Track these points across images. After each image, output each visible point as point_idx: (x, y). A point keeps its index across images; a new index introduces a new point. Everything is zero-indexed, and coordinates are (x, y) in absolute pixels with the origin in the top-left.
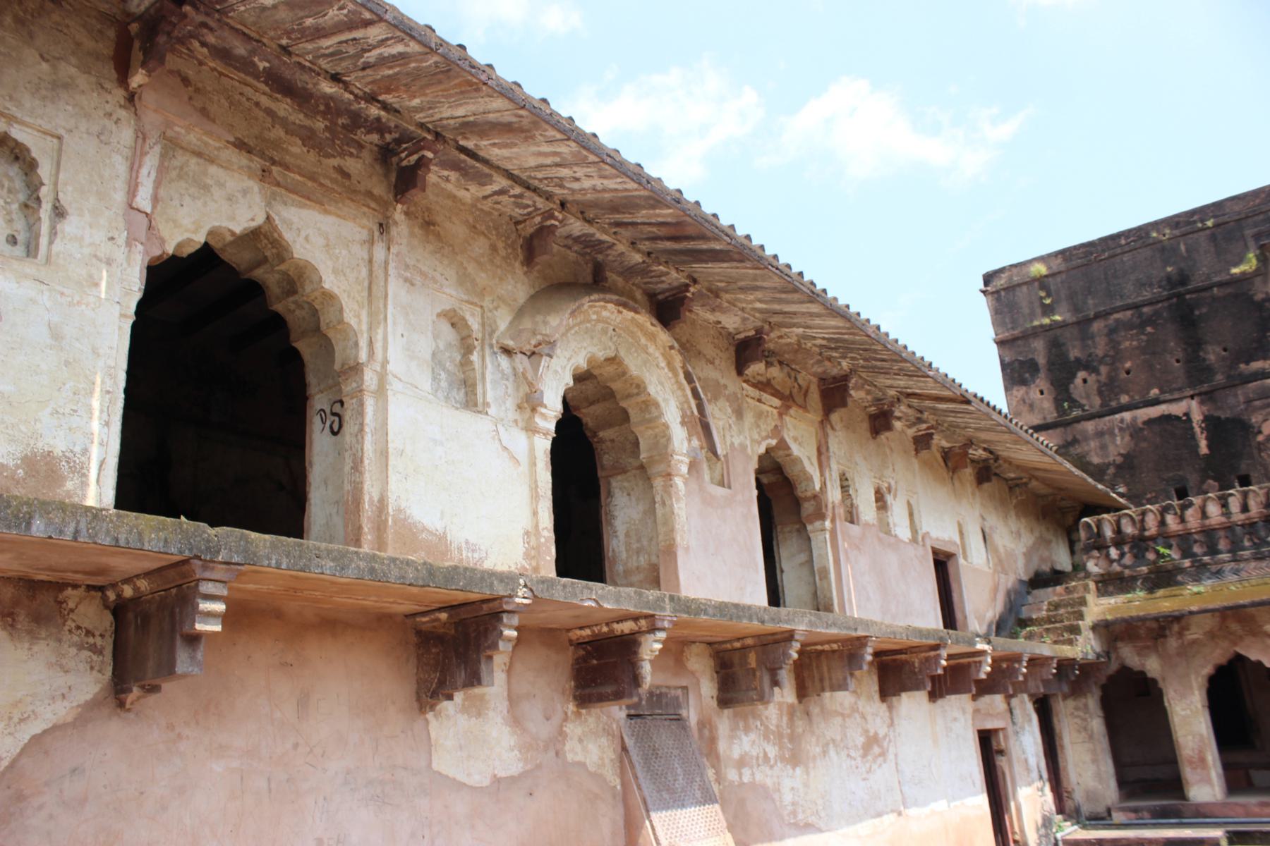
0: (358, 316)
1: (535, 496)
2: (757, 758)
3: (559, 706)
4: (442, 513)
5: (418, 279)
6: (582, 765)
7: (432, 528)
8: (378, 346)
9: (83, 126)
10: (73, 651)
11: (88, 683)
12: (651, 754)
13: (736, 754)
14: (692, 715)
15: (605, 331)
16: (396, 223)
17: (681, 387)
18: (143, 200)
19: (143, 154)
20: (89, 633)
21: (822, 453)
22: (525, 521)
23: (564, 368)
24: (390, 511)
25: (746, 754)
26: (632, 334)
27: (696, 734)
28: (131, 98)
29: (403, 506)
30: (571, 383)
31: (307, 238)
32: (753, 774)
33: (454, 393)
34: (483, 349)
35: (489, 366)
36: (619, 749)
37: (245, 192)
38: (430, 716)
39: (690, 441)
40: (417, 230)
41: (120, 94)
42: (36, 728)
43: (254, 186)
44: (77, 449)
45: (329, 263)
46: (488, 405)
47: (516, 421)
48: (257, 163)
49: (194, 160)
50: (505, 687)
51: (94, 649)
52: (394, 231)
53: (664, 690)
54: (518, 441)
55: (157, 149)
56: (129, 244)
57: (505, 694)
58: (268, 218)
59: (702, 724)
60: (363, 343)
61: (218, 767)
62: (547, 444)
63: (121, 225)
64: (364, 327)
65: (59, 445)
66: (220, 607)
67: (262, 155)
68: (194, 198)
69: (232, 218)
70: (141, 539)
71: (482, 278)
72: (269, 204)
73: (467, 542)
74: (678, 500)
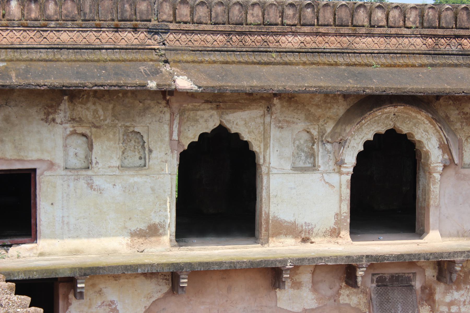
0: (260, 147)
1: (341, 200)
2: (465, 301)
3: (337, 284)
4: (294, 214)
5: (285, 125)
6: (349, 305)
7: (289, 220)
8: (267, 157)
9: (154, 119)
10: (161, 280)
11: (166, 288)
12: (388, 301)
13: (448, 299)
14: (418, 284)
15: (387, 118)
16: (274, 105)
17: (438, 131)
18: (175, 137)
19: (174, 120)
20: (165, 276)
22: (336, 210)
23: (358, 144)
24: (271, 218)
25: (455, 300)
26: (407, 113)
27: (419, 292)
28: (168, 102)
29: (276, 215)
30: (362, 149)
31: (237, 124)
32: (460, 309)
33: (309, 160)
34: (318, 143)
35: (321, 150)
36: (369, 299)
37: (211, 116)
38: (277, 290)
39: (443, 155)
40: (285, 104)
41: (164, 102)
42: (154, 299)
43: (214, 112)
44: (162, 221)
45: (247, 130)
46: (319, 167)
47: (334, 170)
48: (214, 105)
49: (192, 113)
50: (311, 279)
51: (166, 279)
52: (273, 109)
53: (400, 275)
54: (334, 178)
55: (178, 116)
56: (172, 152)
57: (311, 281)
58: (221, 121)
59: (423, 288)
60: (261, 157)
61: (202, 307)
62: (349, 177)
63: (169, 148)
64: (262, 150)
65: (157, 221)
66: (186, 280)
67: (216, 102)
68: (193, 126)
69: (207, 128)
70: (163, 269)
71: (319, 112)
72: (221, 117)
73: (305, 223)
74: (434, 184)
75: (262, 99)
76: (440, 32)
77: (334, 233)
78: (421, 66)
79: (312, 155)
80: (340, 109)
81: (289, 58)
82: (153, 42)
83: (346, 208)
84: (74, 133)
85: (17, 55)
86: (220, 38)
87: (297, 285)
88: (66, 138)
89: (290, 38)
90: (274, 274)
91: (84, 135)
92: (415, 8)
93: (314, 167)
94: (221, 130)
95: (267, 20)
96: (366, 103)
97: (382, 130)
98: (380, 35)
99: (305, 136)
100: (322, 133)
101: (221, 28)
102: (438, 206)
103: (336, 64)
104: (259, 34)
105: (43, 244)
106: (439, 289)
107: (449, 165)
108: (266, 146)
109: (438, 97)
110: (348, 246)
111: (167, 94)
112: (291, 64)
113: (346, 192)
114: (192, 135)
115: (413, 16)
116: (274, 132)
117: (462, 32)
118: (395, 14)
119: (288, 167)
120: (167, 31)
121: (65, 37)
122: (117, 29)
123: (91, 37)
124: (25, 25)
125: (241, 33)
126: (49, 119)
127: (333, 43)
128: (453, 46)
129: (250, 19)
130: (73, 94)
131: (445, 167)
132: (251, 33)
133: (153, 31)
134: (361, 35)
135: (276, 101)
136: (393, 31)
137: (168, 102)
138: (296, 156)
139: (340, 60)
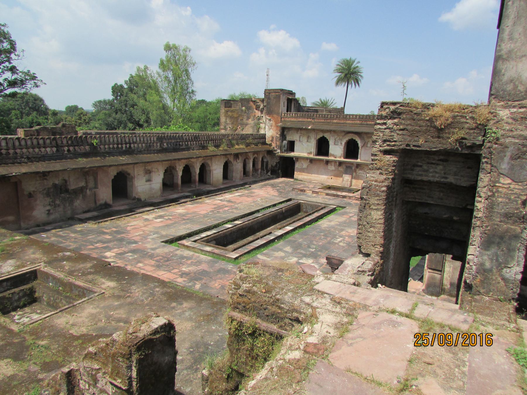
14: (353, 168)
75: (330, 131)
77: (340, 157)
80: (343, 134)
83: (342, 153)
87: (331, 165)
90: (327, 162)
105: (295, 153)
106: (357, 170)
109: (362, 133)
110: (342, 159)
114: (318, 137)
115: (358, 117)
123: (304, 120)
124: (295, 117)
126: (297, 133)
127: (342, 122)
130: (301, 129)
133: (313, 119)
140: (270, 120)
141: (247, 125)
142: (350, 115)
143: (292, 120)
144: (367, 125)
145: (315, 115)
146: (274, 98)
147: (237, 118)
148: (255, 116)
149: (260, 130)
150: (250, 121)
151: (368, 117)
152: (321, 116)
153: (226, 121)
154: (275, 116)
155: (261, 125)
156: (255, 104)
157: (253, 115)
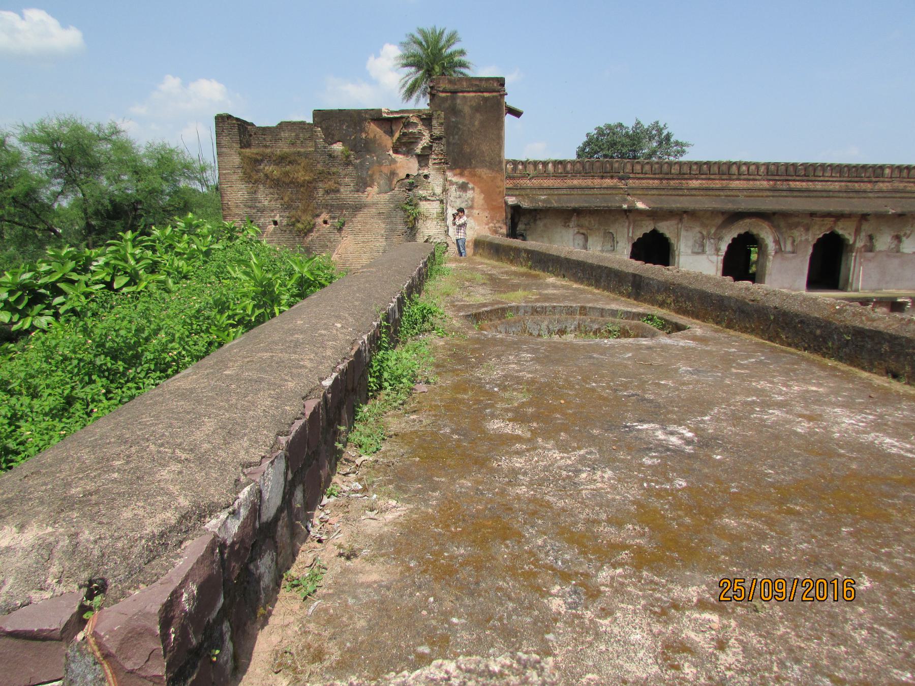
1: (717, 270)
18: (630, 235)
21: (857, 232)
28: (627, 216)
54: (714, 258)
76: (777, 178)
78: (767, 196)
79: (703, 246)
80: (719, 220)
81: (694, 192)
82: (621, 184)
84: (578, 233)
85: (552, 192)
86: (656, 181)
88: (575, 235)
89: (694, 182)
91: (583, 234)
92: (764, 164)
93: (703, 252)
94: (654, 232)
95: (682, 172)
96: (735, 216)
97: (742, 232)
98: (744, 180)
99: (699, 235)
100: (709, 233)
101: (657, 176)
102: (770, 274)
103: (719, 196)
104: (678, 179)
107: (779, 251)
108: (678, 240)
109: (774, 214)
111: (631, 212)
112: (694, 195)
113: (721, 266)
114: (639, 234)
115: (762, 169)
116: (683, 233)
117: (790, 178)
118: (752, 168)
119: (690, 251)
120: (629, 178)
121: (576, 182)
122: (602, 177)
124: (556, 176)
125: (668, 179)
126: (566, 225)
127: (718, 184)
128: (785, 186)
129: (673, 171)
130: (578, 212)
131: (776, 253)
132: (673, 179)
133: (621, 179)
134: (733, 180)
135: (685, 216)
136: (751, 177)
137: (627, 216)
138: (694, 246)
139: (722, 193)
140: (463, 187)
141: (358, 208)
142: (739, 165)
143: (546, 183)
144: (791, 190)
145: (629, 166)
146: (477, 109)
147: (309, 187)
148: (393, 173)
149: (420, 224)
150: (373, 194)
151: (791, 169)
152: (647, 168)
153: (255, 200)
154: (484, 172)
155: (424, 206)
156: (391, 133)
157: (386, 170)
